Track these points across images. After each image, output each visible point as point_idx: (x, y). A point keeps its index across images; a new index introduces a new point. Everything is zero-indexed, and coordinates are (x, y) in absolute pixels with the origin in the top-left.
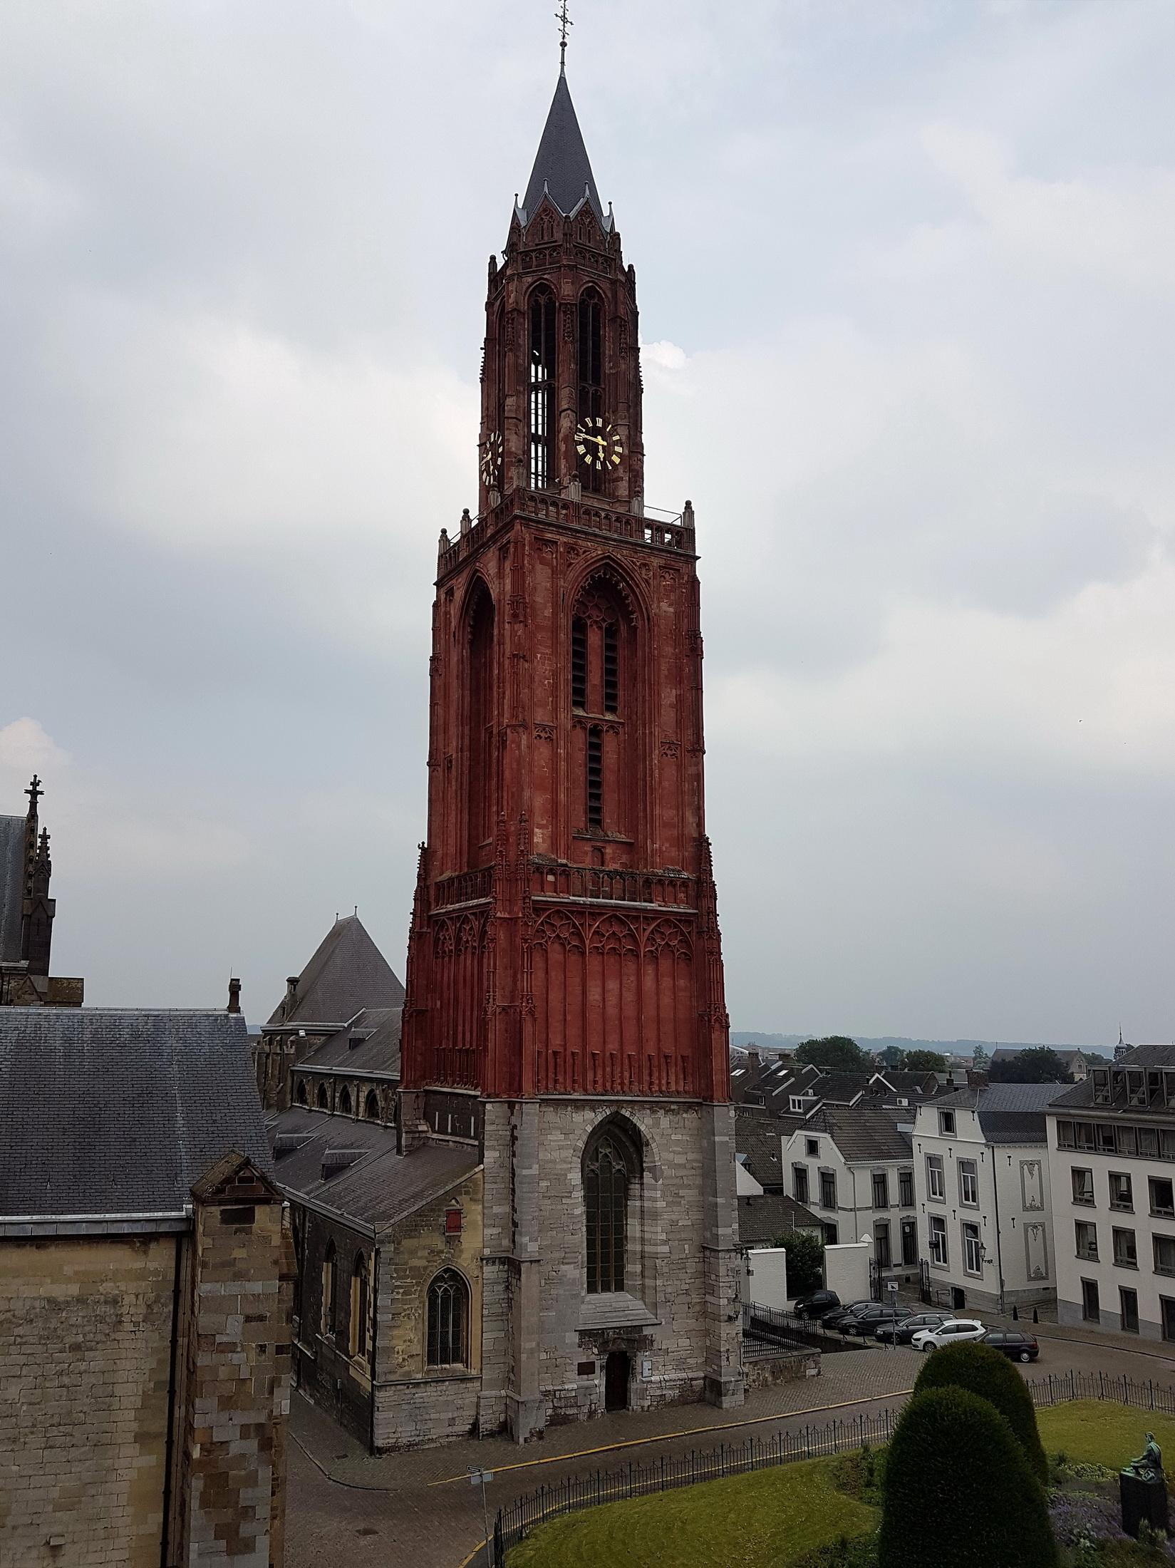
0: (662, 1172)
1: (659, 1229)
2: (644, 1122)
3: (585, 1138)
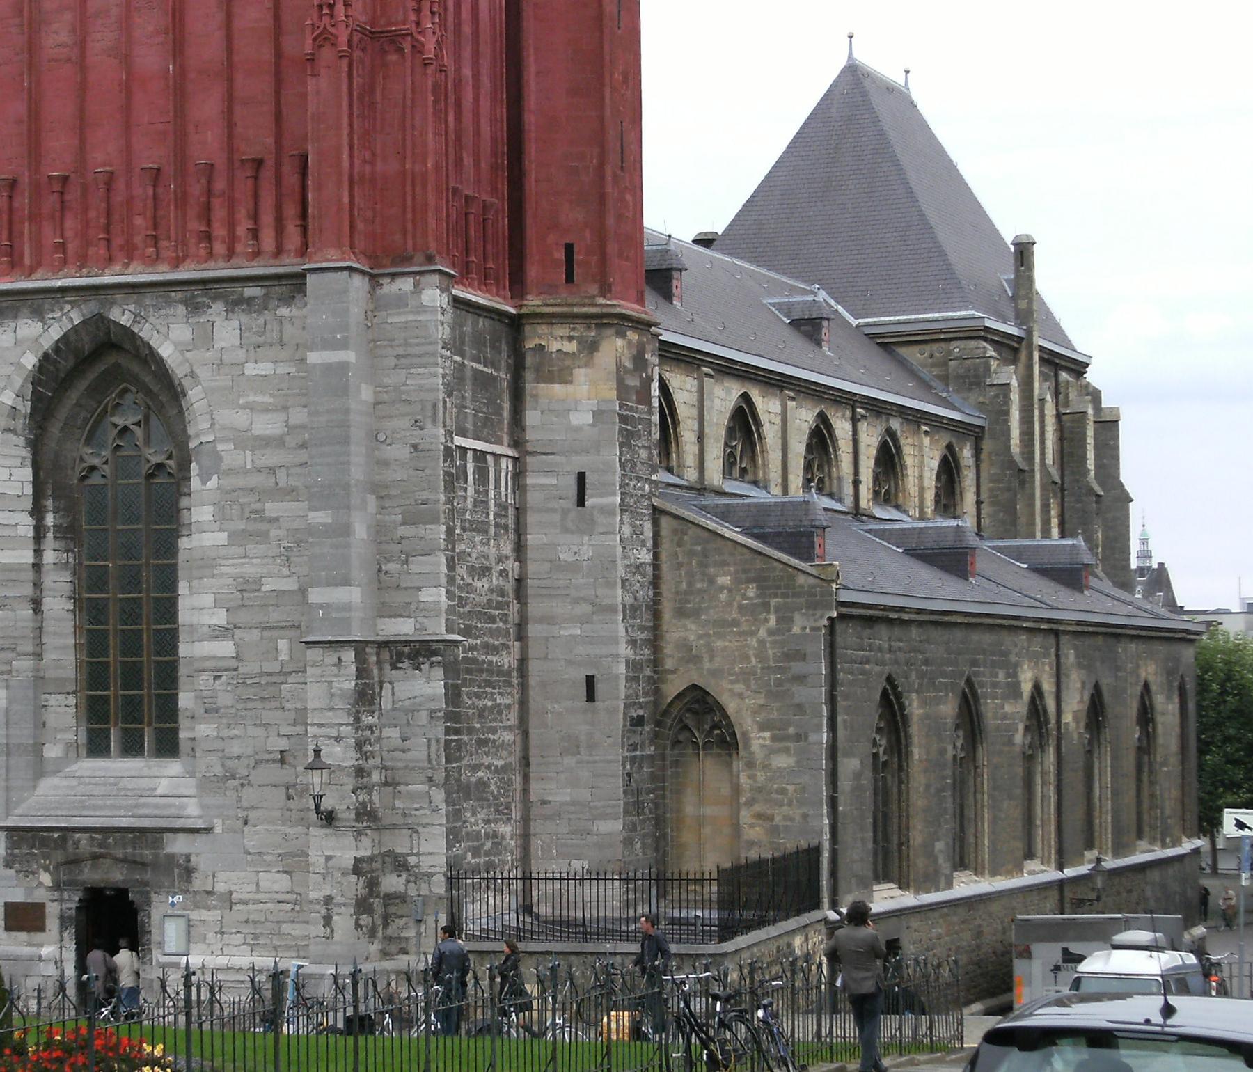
0: (218, 458)
1: (208, 600)
2: (170, 337)
3: (18, 382)
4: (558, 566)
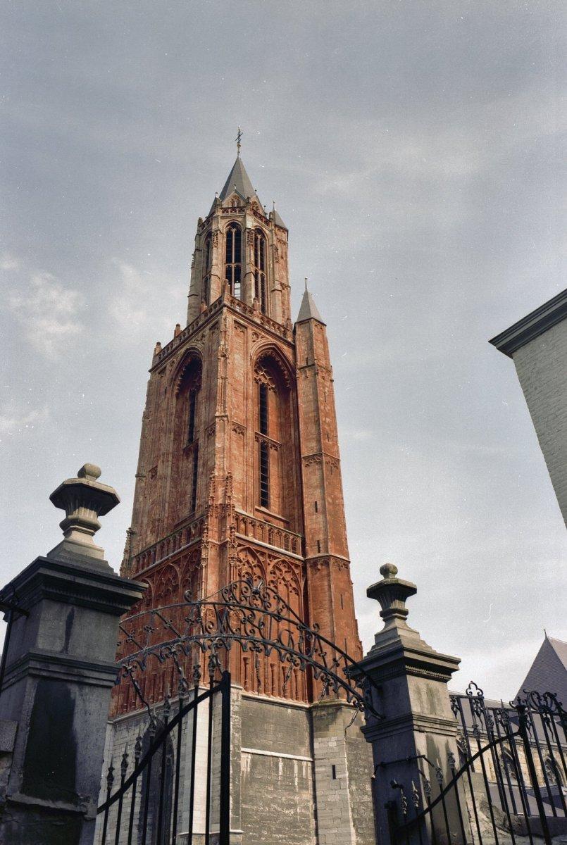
4: (327, 803)
